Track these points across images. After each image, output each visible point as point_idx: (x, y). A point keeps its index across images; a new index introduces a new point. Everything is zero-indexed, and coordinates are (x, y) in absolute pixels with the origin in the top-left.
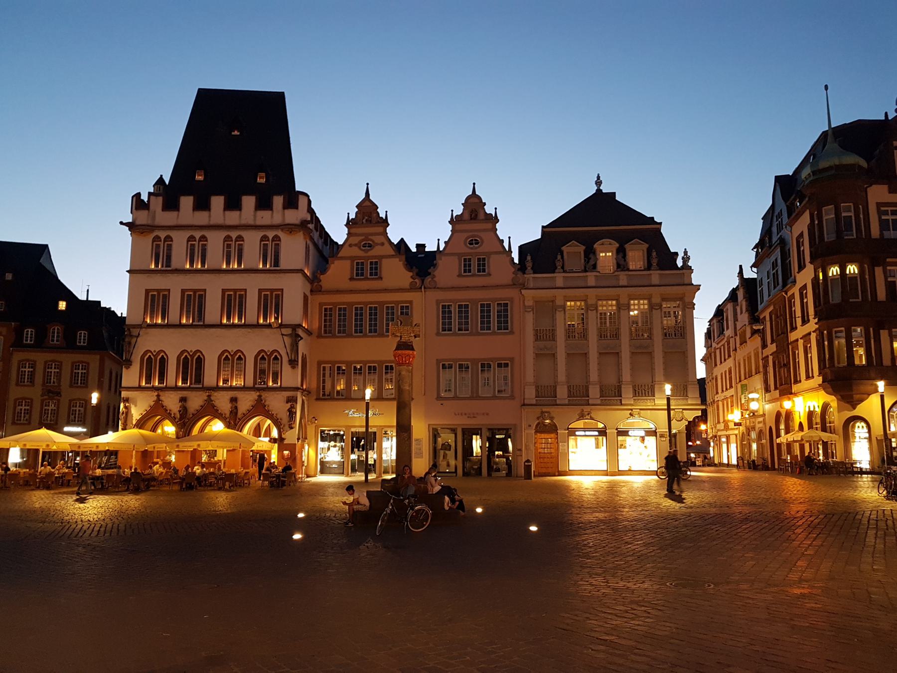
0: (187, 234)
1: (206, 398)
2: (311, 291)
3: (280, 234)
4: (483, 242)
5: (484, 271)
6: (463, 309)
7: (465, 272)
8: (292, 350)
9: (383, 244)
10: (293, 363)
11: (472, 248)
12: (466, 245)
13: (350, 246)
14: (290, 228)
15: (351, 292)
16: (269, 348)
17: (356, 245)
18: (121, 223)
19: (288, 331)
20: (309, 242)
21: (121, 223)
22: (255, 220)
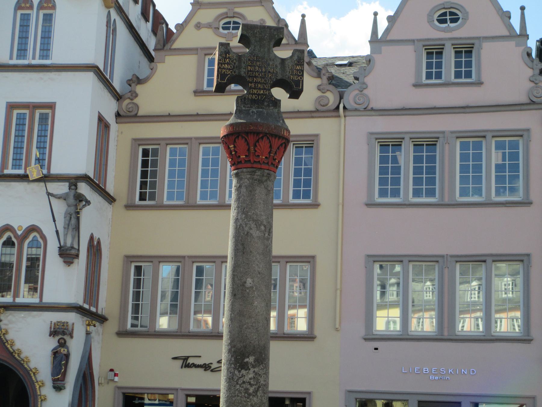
2: (118, 115)
4: (465, 19)
5: (468, 75)
6: (427, 145)
7: (429, 76)
10: (68, 255)
11: (444, 30)
12: (430, 21)
13: (198, 26)
16: (20, 223)
17: (209, 26)
19: (62, 188)
20: (114, 15)
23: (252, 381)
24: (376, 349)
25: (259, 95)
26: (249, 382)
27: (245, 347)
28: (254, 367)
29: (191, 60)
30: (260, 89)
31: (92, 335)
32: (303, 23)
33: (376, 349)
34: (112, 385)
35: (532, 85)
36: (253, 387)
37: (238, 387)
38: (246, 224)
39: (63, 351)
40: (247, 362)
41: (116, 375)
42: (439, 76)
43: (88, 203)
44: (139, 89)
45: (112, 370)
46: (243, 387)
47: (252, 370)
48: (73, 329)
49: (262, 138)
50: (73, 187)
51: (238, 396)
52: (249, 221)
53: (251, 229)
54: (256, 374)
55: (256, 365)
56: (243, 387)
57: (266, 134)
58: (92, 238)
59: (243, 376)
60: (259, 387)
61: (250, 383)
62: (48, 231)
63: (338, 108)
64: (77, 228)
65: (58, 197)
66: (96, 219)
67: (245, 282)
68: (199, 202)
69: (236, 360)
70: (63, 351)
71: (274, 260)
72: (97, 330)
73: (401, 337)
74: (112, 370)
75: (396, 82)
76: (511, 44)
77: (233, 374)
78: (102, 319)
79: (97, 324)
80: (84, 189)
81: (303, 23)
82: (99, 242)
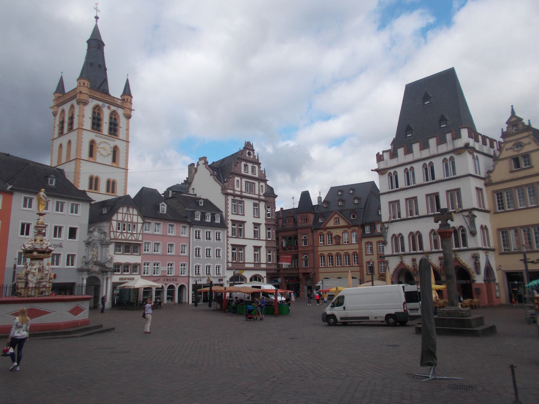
0: (403, 168)
3: (452, 155)
9: (530, 143)
14: (458, 151)
15: (512, 180)
17: (511, 149)
18: (372, 170)
19: (466, 214)
21: (372, 170)
22: (438, 151)
29: (506, 162)
43: (476, 216)
44: (491, 175)
62: (466, 227)
65: (467, 216)
68: (519, 207)
82: (486, 226)
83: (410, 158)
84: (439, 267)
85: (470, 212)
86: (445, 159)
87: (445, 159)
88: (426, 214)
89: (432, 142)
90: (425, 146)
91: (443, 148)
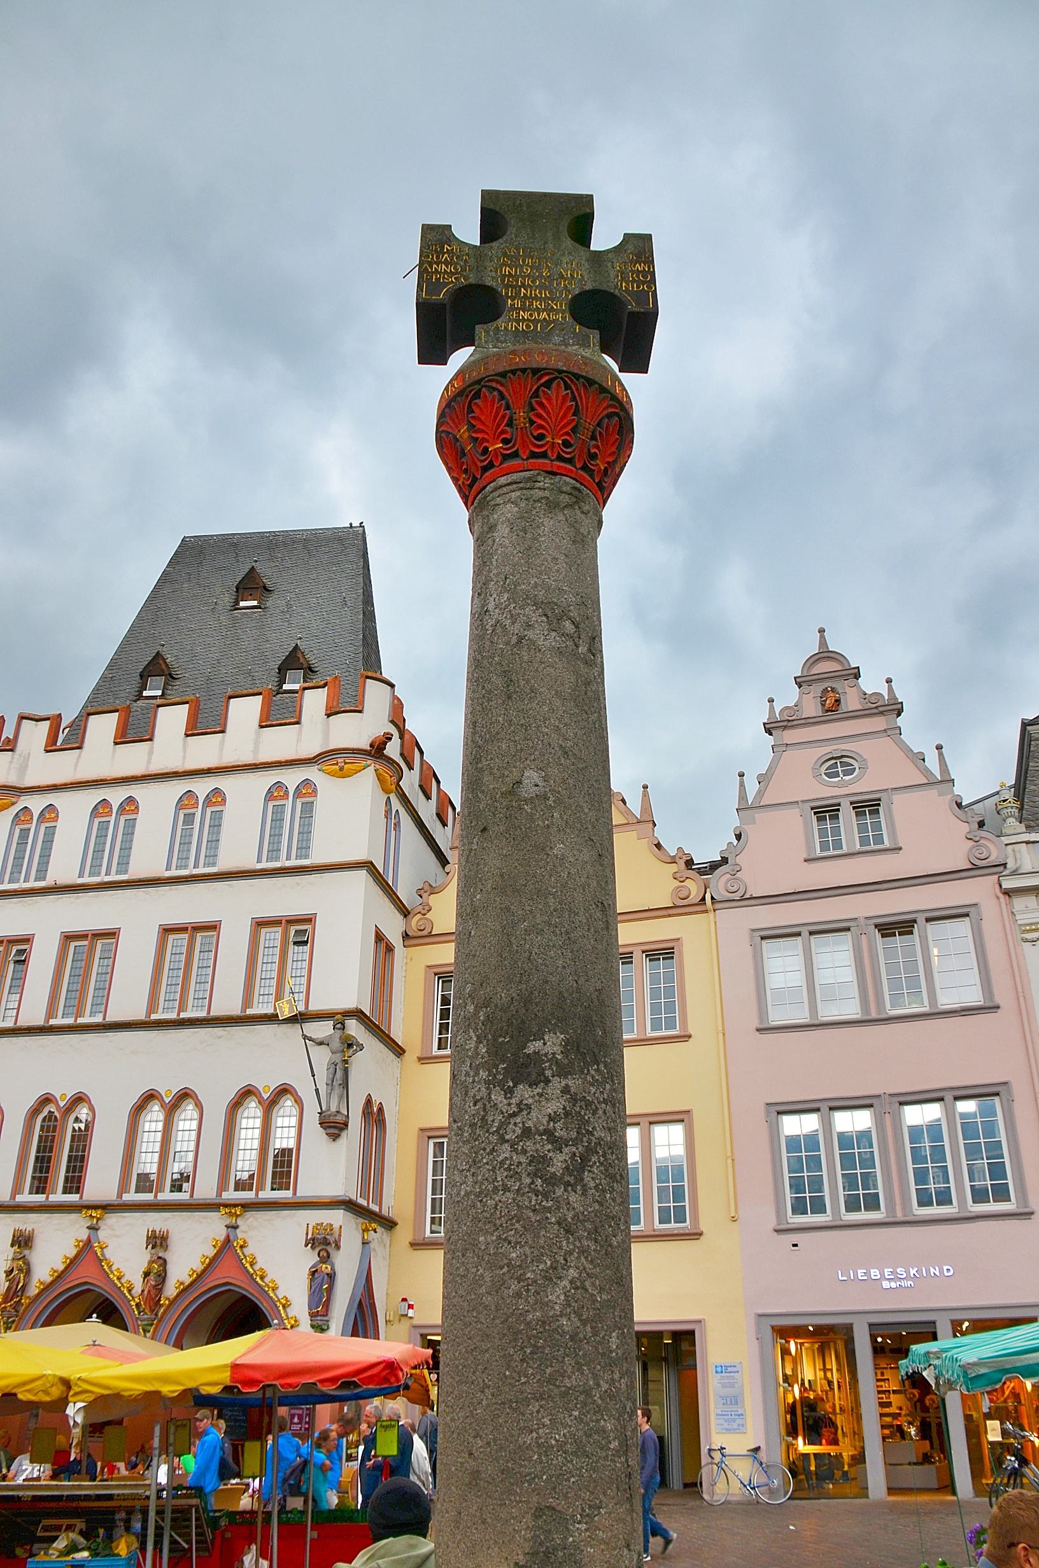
1: (84, 1234)
2: (406, 936)
3: (312, 773)
8: (330, 1084)
10: (334, 1127)
19: (324, 1029)
20: (396, 804)
23: (558, 1125)
24: (795, 1245)
25: (535, 322)
26: (547, 1132)
27: (527, 1001)
28: (563, 1071)
30: (538, 310)
31: (372, 1245)
32: (645, 795)
33: (795, 1245)
34: (405, 1325)
35: (971, 843)
36: (566, 1150)
37: (505, 1151)
38: (514, 618)
39: (326, 1268)
40: (536, 1053)
41: (411, 1307)
42: (838, 844)
44: (433, 900)
45: (404, 1300)
46: (524, 1152)
47: (557, 1084)
48: (340, 1235)
49: (548, 385)
50: (339, 1026)
51: (506, 1189)
52: (522, 608)
53: (529, 626)
54: (574, 1100)
55: (571, 1063)
56: (524, 1152)
57: (560, 372)
58: (369, 1101)
59: (522, 1107)
60: (590, 1150)
61: (549, 1133)
63: (704, 899)
64: (345, 1084)
66: (372, 1072)
67: (519, 782)
69: (496, 1051)
70: (326, 1268)
71: (628, 1121)
72: (378, 1236)
73: (832, 1224)
74: (404, 1300)
75: (781, 855)
76: (933, 792)
77: (487, 1105)
78: (389, 1224)
79: (379, 1229)
80: (354, 1028)
81: (645, 795)
82: (381, 1109)
83: (134, 759)
84: (138, 1288)
85: (341, 1026)
86: (279, 785)
87: (279, 785)
88: (138, 1013)
89: (245, 712)
90: (205, 722)
91: (281, 742)
